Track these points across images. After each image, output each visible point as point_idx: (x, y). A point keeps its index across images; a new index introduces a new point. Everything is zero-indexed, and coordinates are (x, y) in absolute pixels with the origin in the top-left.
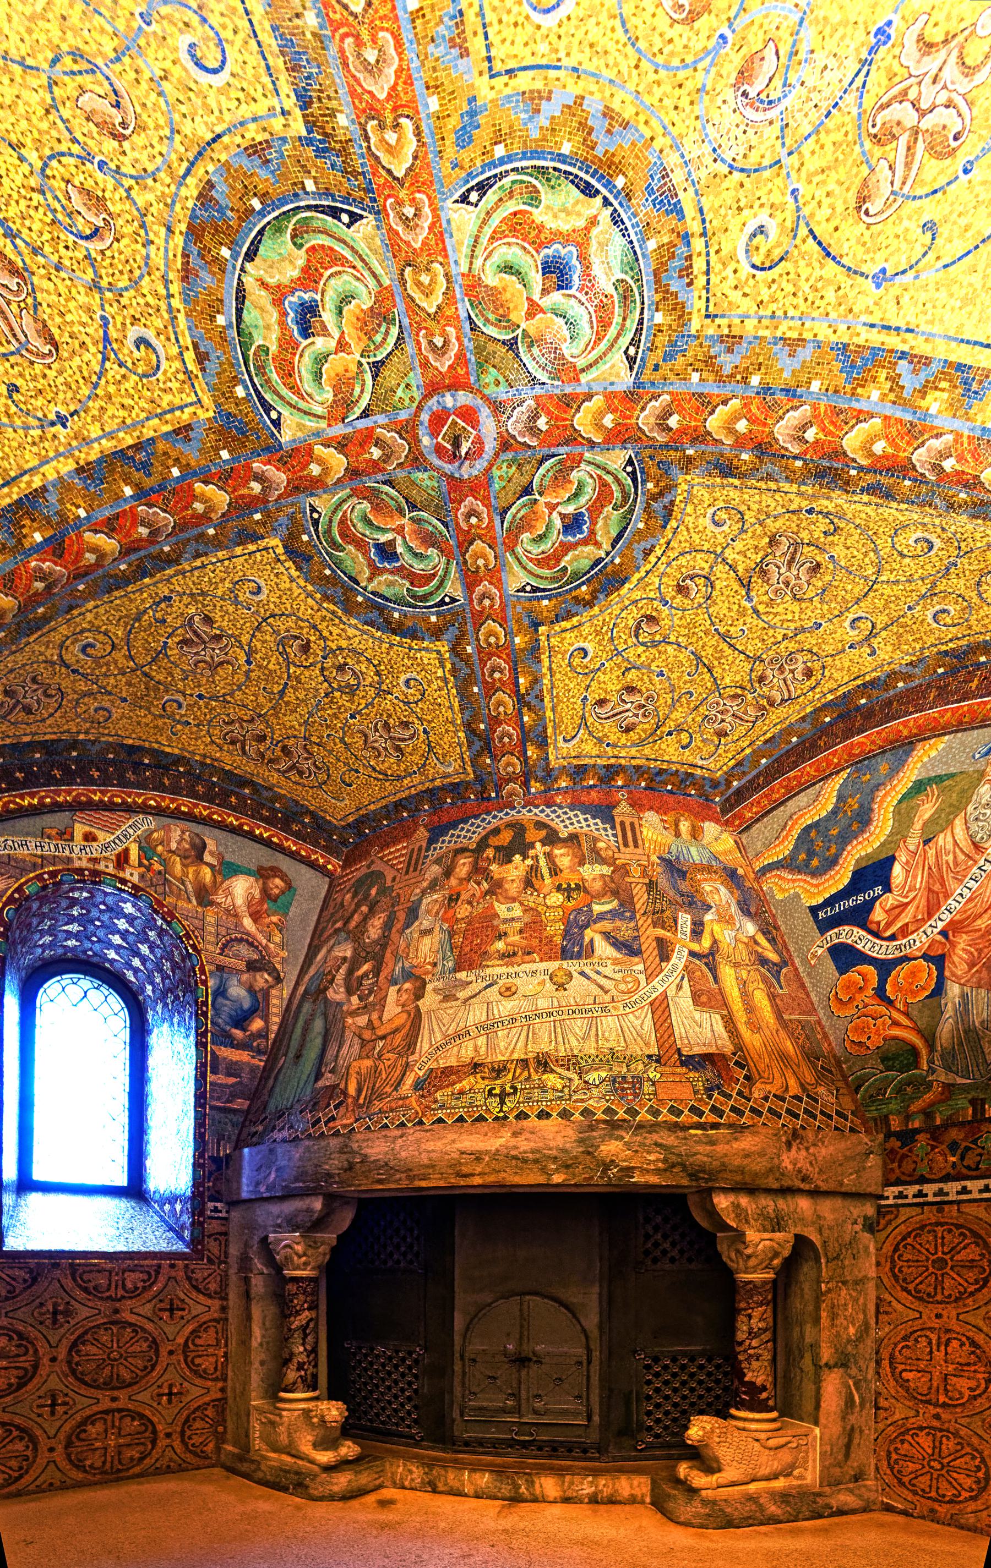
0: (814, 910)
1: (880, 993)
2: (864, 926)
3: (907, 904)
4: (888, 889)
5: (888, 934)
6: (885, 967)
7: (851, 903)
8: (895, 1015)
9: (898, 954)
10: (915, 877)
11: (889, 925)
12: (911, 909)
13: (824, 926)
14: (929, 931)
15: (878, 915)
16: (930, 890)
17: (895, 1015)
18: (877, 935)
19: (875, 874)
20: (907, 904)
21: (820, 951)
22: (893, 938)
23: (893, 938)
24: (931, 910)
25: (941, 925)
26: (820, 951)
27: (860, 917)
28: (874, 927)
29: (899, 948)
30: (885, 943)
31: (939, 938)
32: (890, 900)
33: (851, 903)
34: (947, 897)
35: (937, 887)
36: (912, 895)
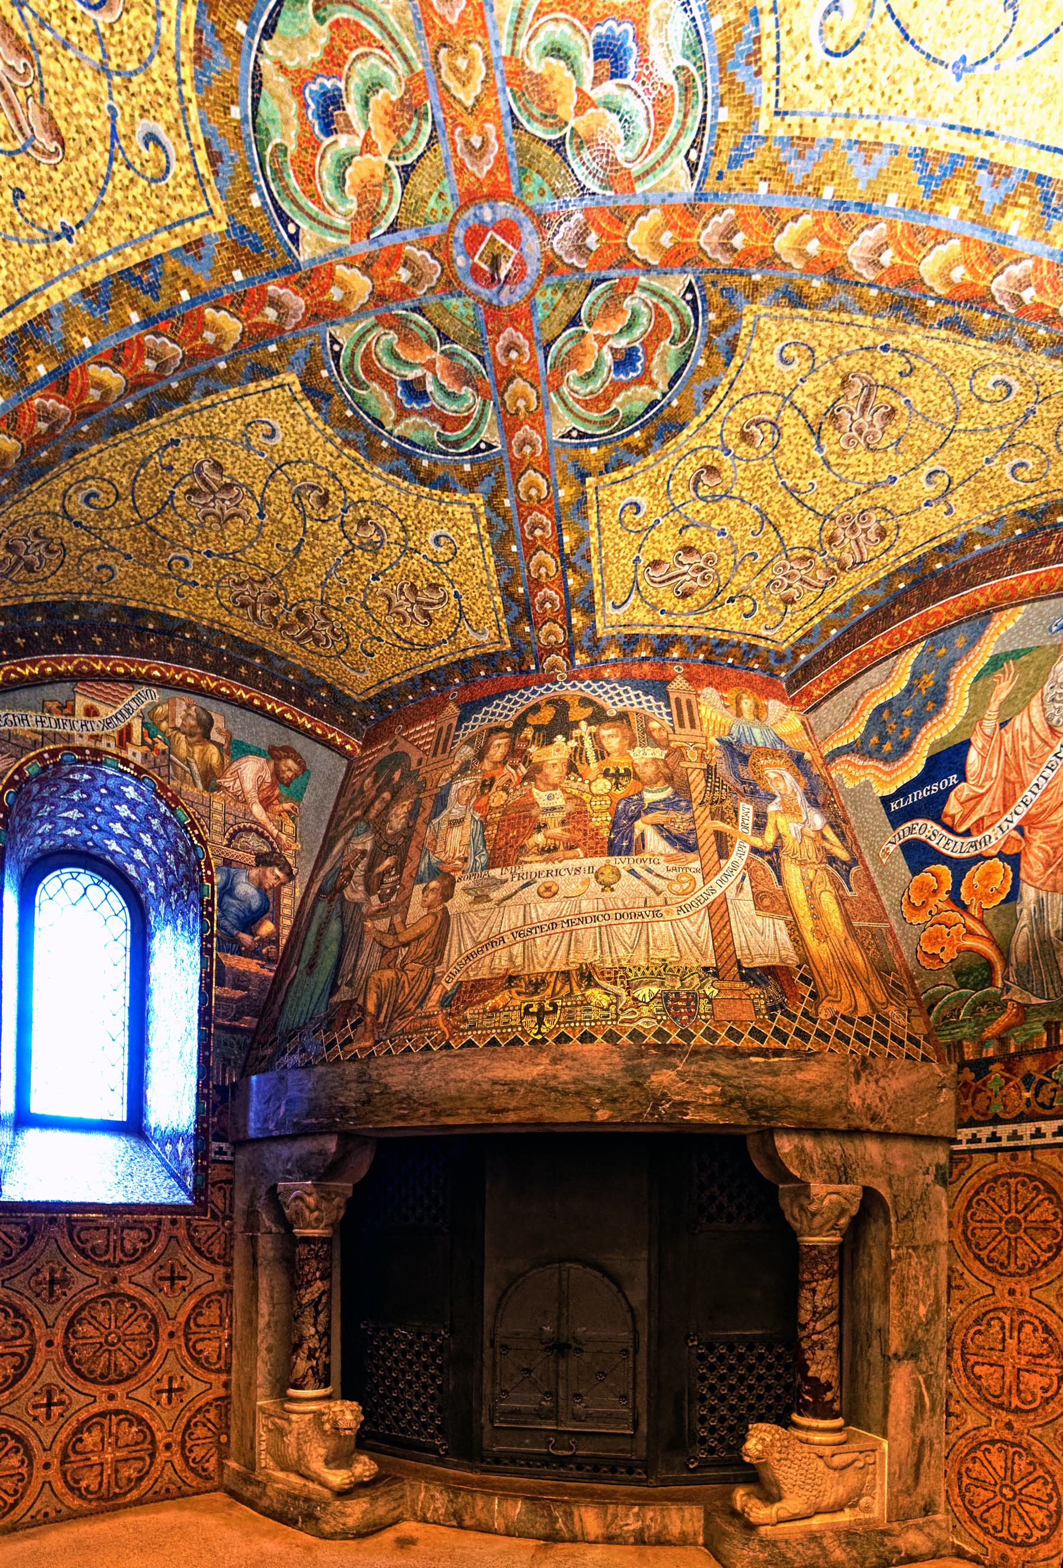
1: (955, 897)
2: (938, 820)
3: (982, 795)
4: (963, 778)
5: (962, 829)
6: (960, 867)
7: (924, 793)
8: (970, 923)
9: (973, 852)
10: (991, 765)
11: (964, 818)
12: (987, 801)
13: (897, 819)
14: (1005, 825)
15: (953, 807)
17: (970, 923)
18: (951, 830)
20: (982, 795)
21: (892, 848)
22: (967, 833)
25: (1017, 819)
27: (933, 809)
29: (973, 845)
30: (959, 840)
31: (1015, 834)
32: (965, 790)
33: (924, 793)
34: (1023, 787)
35: (1013, 776)
36: (987, 785)
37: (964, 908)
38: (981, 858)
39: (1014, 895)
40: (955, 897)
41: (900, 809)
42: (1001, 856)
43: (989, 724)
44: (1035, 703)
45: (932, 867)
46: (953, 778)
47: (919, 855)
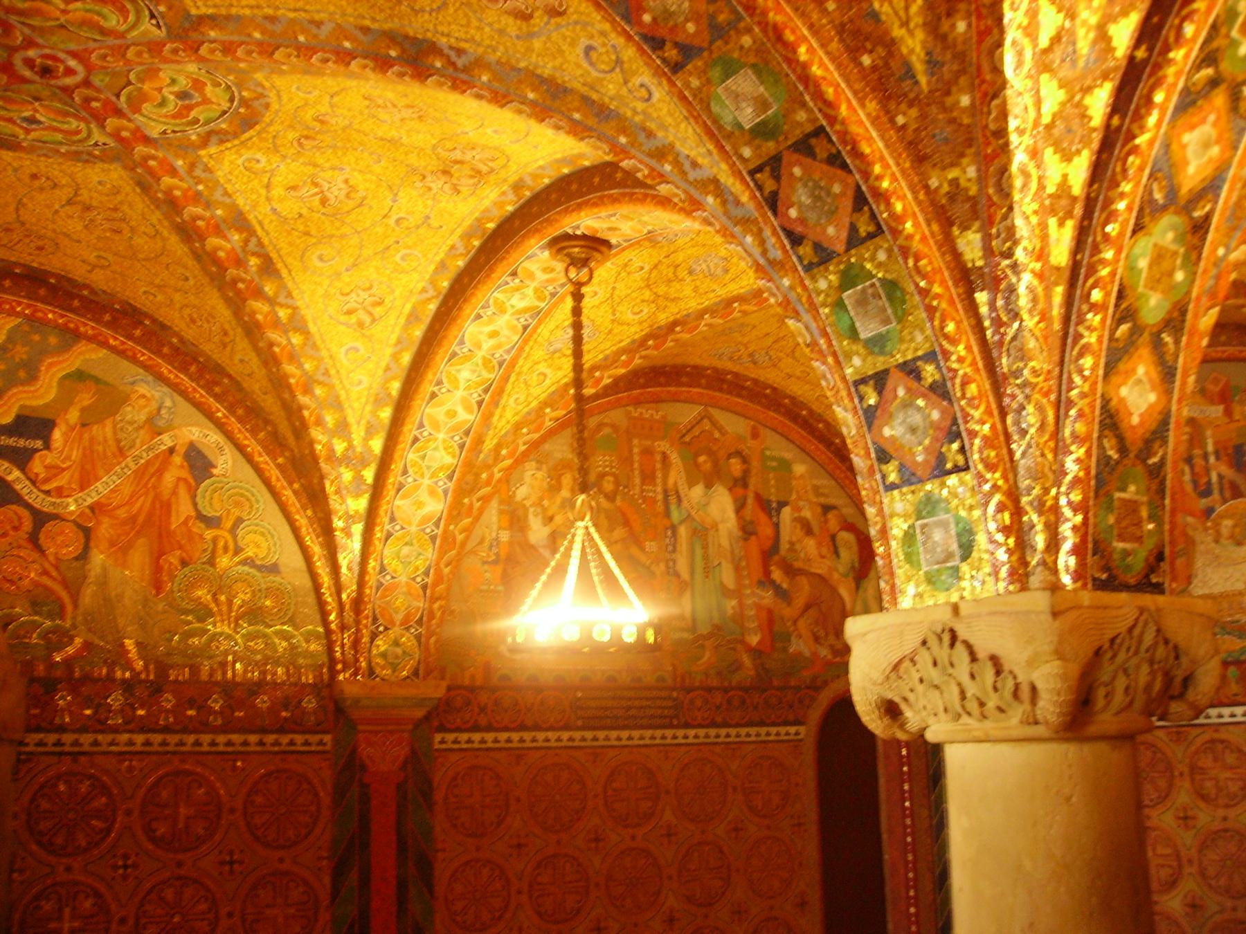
1: (34, 539)
2: (23, 470)
3: (64, 470)
4: (47, 447)
5: (46, 487)
6: (41, 519)
7: (11, 441)
10: (71, 449)
11: (46, 480)
14: (80, 501)
15: (37, 466)
16: (83, 468)
17: (47, 565)
18: (34, 483)
20: (64, 470)
22: (48, 493)
23: (48, 493)
25: (90, 501)
27: (21, 459)
28: (33, 477)
30: (42, 496)
31: (87, 511)
32: (50, 458)
33: (11, 441)
34: (98, 479)
35: (88, 467)
37: (42, 552)
38: (56, 517)
39: (84, 556)
42: (74, 521)
43: (73, 416)
44: (109, 423)
45: (14, 507)
46: (39, 444)
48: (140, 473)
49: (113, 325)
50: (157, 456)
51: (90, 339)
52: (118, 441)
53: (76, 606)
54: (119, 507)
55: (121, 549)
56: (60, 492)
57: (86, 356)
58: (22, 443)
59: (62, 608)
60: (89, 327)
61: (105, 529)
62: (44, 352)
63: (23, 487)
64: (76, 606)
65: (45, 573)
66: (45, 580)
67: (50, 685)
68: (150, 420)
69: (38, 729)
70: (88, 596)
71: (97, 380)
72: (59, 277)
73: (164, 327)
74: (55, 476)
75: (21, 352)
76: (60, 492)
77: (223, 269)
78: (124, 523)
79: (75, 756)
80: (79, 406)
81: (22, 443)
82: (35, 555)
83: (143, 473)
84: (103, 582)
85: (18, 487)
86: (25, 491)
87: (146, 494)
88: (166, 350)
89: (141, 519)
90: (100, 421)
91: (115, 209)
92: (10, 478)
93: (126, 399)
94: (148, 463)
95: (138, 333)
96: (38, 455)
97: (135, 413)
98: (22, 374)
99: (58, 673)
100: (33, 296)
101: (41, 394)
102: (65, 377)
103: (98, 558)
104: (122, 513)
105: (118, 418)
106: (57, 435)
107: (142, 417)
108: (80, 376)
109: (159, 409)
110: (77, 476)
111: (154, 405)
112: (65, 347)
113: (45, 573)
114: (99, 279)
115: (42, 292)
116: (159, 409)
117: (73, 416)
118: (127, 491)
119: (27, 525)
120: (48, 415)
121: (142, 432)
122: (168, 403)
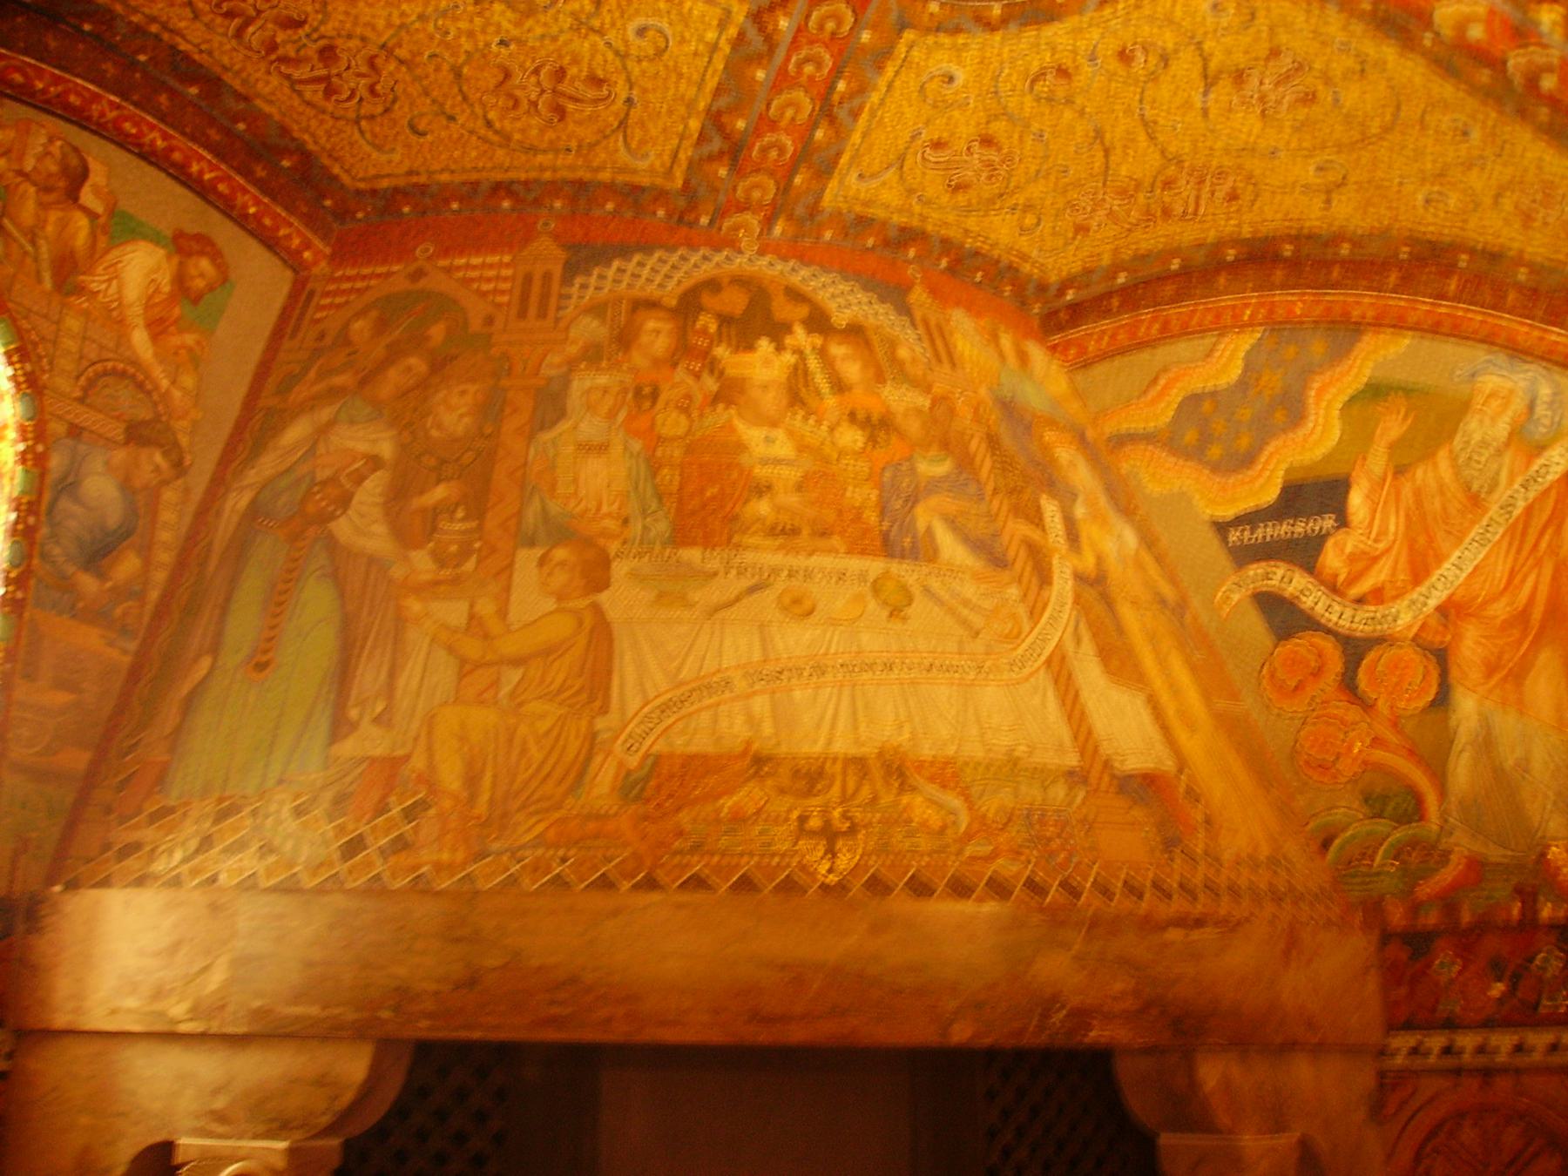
0: (1222, 528)
1: (1348, 685)
4: (1343, 522)
6: (1354, 649)
7: (1283, 529)
10: (1385, 521)
11: (1353, 579)
13: (1244, 556)
15: (1332, 559)
16: (1411, 548)
19: (1317, 495)
22: (1360, 601)
24: (1419, 571)
25: (1433, 603)
26: (1236, 597)
27: (1305, 554)
32: (1351, 541)
33: (1283, 529)
34: (1440, 559)
37: (1368, 707)
38: (1380, 640)
39: (1442, 700)
40: (1348, 685)
41: (1244, 540)
44: (1442, 456)
46: (1328, 522)
47: (1283, 616)
48: (1519, 531)
49: (1407, 283)
50: (1546, 493)
51: (1378, 324)
52: (1467, 487)
53: (1443, 793)
54: (1494, 599)
55: (1510, 676)
56: (1377, 596)
57: (1381, 355)
58: (1300, 528)
59: (1419, 801)
60: (1363, 302)
61: (1471, 646)
62: (1307, 373)
63: (1314, 599)
64: (1443, 793)
65: (1377, 742)
66: (1379, 755)
67: (1418, 942)
68: (1517, 434)
69: (1409, 1026)
70: (1462, 771)
71: (1407, 391)
72: (1296, 239)
73: (1494, 257)
74: (1367, 569)
75: (1273, 381)
76: (1377, 596)
77: (1499, 65)
78: (1507, 625)
79: (1487, 1074)
80: (1383, 443)
81: (1300, 528)
82: (1353, 714)
83: (1524, 534)
84: (1486, 743)
85: (1307, 602)
86: (1320, 608)
87: (1539, 563)
88: (1512, 296)
89: (1537, 614)
90: (1428, 455)
91: (1275, 53)
92: (1290, 591)
93: (1463, 407)
94: (1529, 510)
95: (1453, 285)
96: (1330, 544)
97: (1485, 428)
98: (1279, 416)
99: (1431, 918)
100: (1264, 286)
101: (1316, 440)
102: (1352, 399)
103: (1467, 706)
104: (1500, 610)
105: (1458, 442)
106: (1356, 500)
107: (1502, 429)
108: (1375, 392)
109: (1531, 407)
110: (1403, 559)
111: (1518, 405)
112: (1339, 353)
113: (1377, 742)
114: (1347, 213)
115: (1279, 275)
116: (1531, 407)
117: (1378, 461)
118: (1501, 569)
119: (1335, 664)
120: (1331, 470)
121: (1507, 458)
122: (1545, 391)
